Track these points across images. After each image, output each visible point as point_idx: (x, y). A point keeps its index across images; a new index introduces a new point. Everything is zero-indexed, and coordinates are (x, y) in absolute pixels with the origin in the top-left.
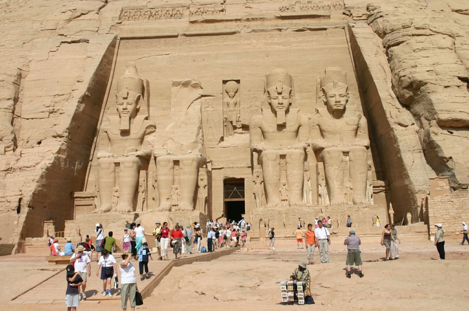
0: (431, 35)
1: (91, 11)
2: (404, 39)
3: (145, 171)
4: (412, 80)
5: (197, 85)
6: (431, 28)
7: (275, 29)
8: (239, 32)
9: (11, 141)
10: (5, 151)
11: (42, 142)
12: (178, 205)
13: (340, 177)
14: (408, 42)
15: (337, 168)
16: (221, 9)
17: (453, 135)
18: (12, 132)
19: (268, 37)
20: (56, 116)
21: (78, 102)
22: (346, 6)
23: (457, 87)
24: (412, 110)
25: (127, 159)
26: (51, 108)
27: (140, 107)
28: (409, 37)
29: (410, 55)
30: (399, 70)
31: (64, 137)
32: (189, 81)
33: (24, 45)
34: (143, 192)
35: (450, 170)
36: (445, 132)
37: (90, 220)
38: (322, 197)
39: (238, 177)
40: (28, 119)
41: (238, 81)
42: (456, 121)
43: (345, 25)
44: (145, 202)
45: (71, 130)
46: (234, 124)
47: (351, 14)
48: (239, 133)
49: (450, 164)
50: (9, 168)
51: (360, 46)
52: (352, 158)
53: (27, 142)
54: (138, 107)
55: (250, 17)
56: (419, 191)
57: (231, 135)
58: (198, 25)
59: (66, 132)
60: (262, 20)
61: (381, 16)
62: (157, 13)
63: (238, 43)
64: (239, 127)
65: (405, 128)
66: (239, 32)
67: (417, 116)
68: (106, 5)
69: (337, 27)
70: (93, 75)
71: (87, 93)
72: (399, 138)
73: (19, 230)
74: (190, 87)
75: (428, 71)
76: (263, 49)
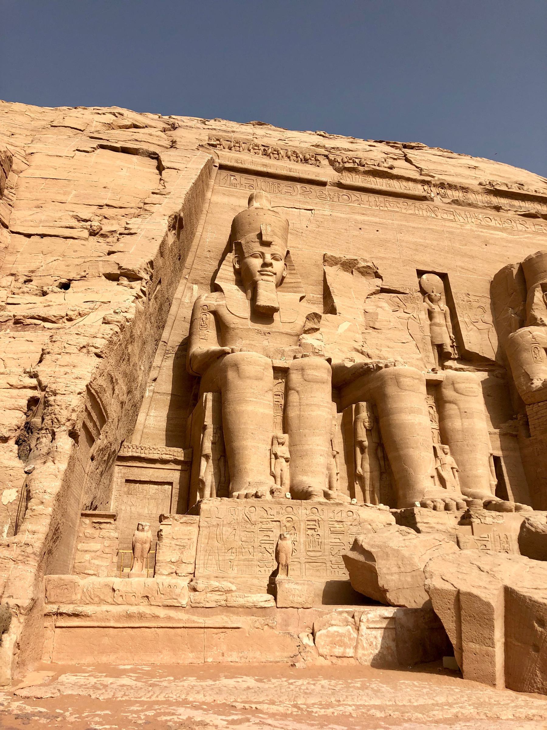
8: (432, 200)
11: (71, 285)
19: (480, 216)
26: (95, 224)
31: (140, 279)
32: (356, 260)
37: (254, 518)
41: (444, 277)
48: (456, 370)
54: (285, 274)
58: (357, 176)
60: (464, 190)
62: (276, 152)
63: (433, 215)
64: (457, 357)
66: (432, 200)
71: (182, 215)
76: (476, 233)
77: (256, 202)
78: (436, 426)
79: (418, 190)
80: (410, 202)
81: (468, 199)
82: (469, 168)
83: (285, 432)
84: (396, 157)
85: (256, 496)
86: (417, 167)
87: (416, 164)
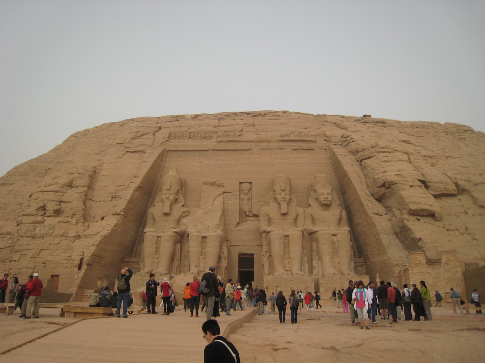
0: (392, 152)
1: (149, 133)
2: (374, 154)
3: (180, 244)
4: (385, 181)
6: (392, 148)
7: (278, 149)
8: (252, 149)
9: (81, 216)
10: (77, 223)
12: (204, 271)
13: (331, 254)
14: (377, 156)
15: (328, 246)
16: (239, 134)
17: (420, 221)
18: (83, 210)
20: (117, 200)
21: (134, 191)
22: (327, 135)
23: (419, 187)
24: (384, 204)
25: (166, 233)
26: (114, 194)
27: (178, 198)
28: (377, 153)
29: (380, 164)
30: (373, 175)
31: (120, 215)
33: (101, 153)
34: (177, 260)
36: (414, 218)
38: (316, 269)
39: (249, 252)
40: (97, 201)
42: (423, 210)
43: (326, 147)
44: (179, 268)
45: (127, 210)
46: (247, 213)
47: (331, 141)
50: (78, 236)
51: (340, 160)
53: (94, 218)
55: (260, 140)
56: (396, 264)
57: (244, 222)
59: (122, 211)
60: (268, 142)
61: (353, 141)
62: (194, 136)
65: (380, 217)
66: (252, 149)
67: (388, 209)
68: (159, 130)
70: (146, 173)
71: (140, 185)
72: (377, 224)
73: (77, 283)
75: (396, 175)
80: (242, 152)
82: (283, 124)
84: (248, 126)
87: (256, 128)
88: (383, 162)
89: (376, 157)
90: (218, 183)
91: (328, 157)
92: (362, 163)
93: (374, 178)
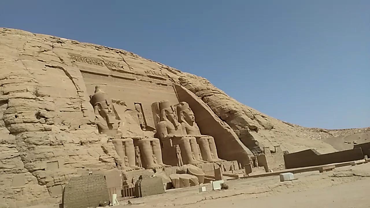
5: (123, 104)
16: (122, 66)
22: (170, 77)
30: (221, 106)
35: (256, 145)
41: (140, 104)
47: (173, 81)
49: (256, 143)
52: (211, 142)
61: (190, 84)
64: (145, 127)
65: (229, 130)
66: (135, 80)
69: (170, 85)
72: (232, 133)
74: (120, 104)
77: (100, 89)
78: (152, 151)
79: (131, 76)
81: (143, 78)
82: (140, 63)
83: (126, 156)
84: (121, 60)
85: (131, 170)
86: (128, 64)
88: (220, 99)
89: (215, 96)
90: (121, 102)
91: (175, 91)
92: (205, 98)
93: (223, 108)
